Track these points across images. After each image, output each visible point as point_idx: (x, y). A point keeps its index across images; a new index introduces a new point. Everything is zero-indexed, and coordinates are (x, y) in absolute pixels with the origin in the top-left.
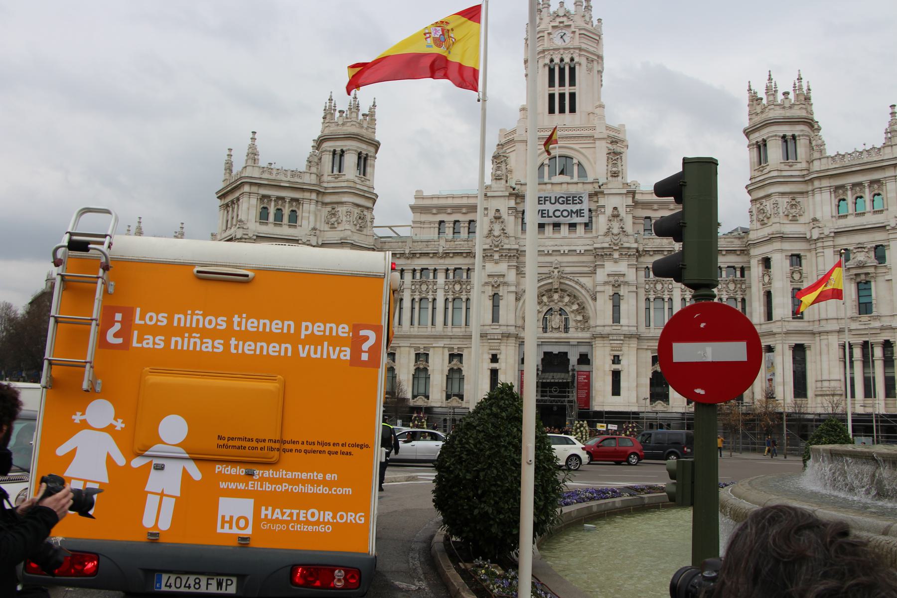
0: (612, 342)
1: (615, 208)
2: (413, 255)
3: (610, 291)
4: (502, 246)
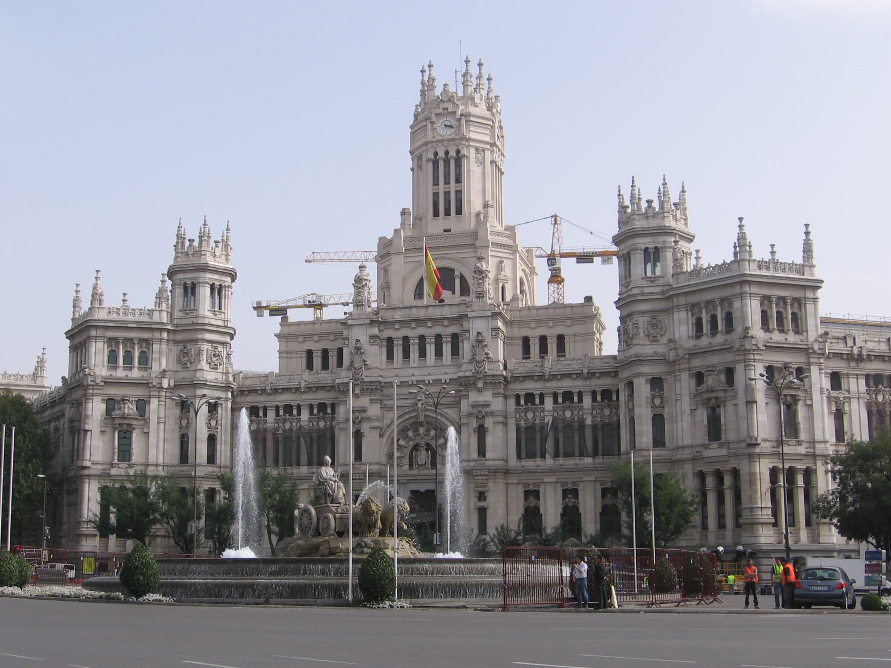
0: (476, 478)
1: (479, 333)
2: (275, 391)
3: (474, 424)
4: (363, 379)
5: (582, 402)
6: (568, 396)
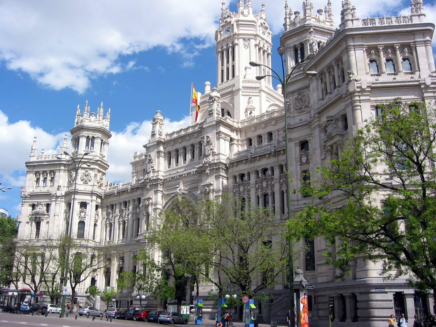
5: (273, 175)
6: (265, 171)
